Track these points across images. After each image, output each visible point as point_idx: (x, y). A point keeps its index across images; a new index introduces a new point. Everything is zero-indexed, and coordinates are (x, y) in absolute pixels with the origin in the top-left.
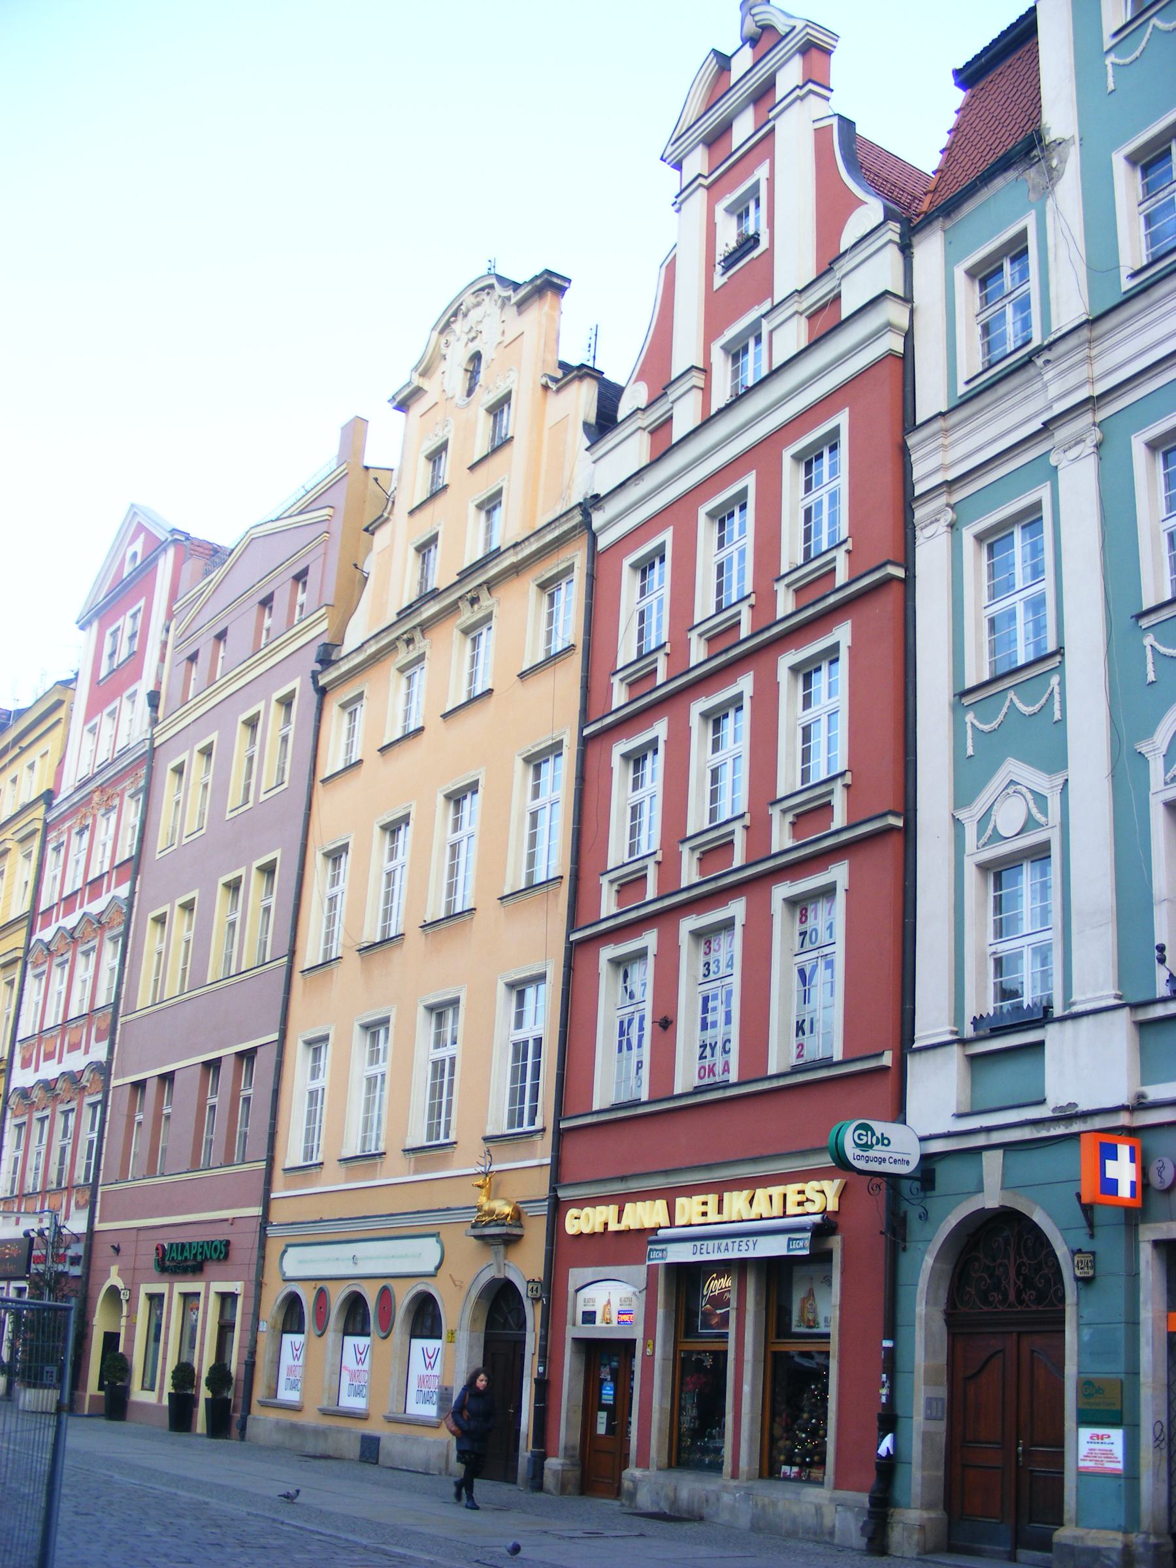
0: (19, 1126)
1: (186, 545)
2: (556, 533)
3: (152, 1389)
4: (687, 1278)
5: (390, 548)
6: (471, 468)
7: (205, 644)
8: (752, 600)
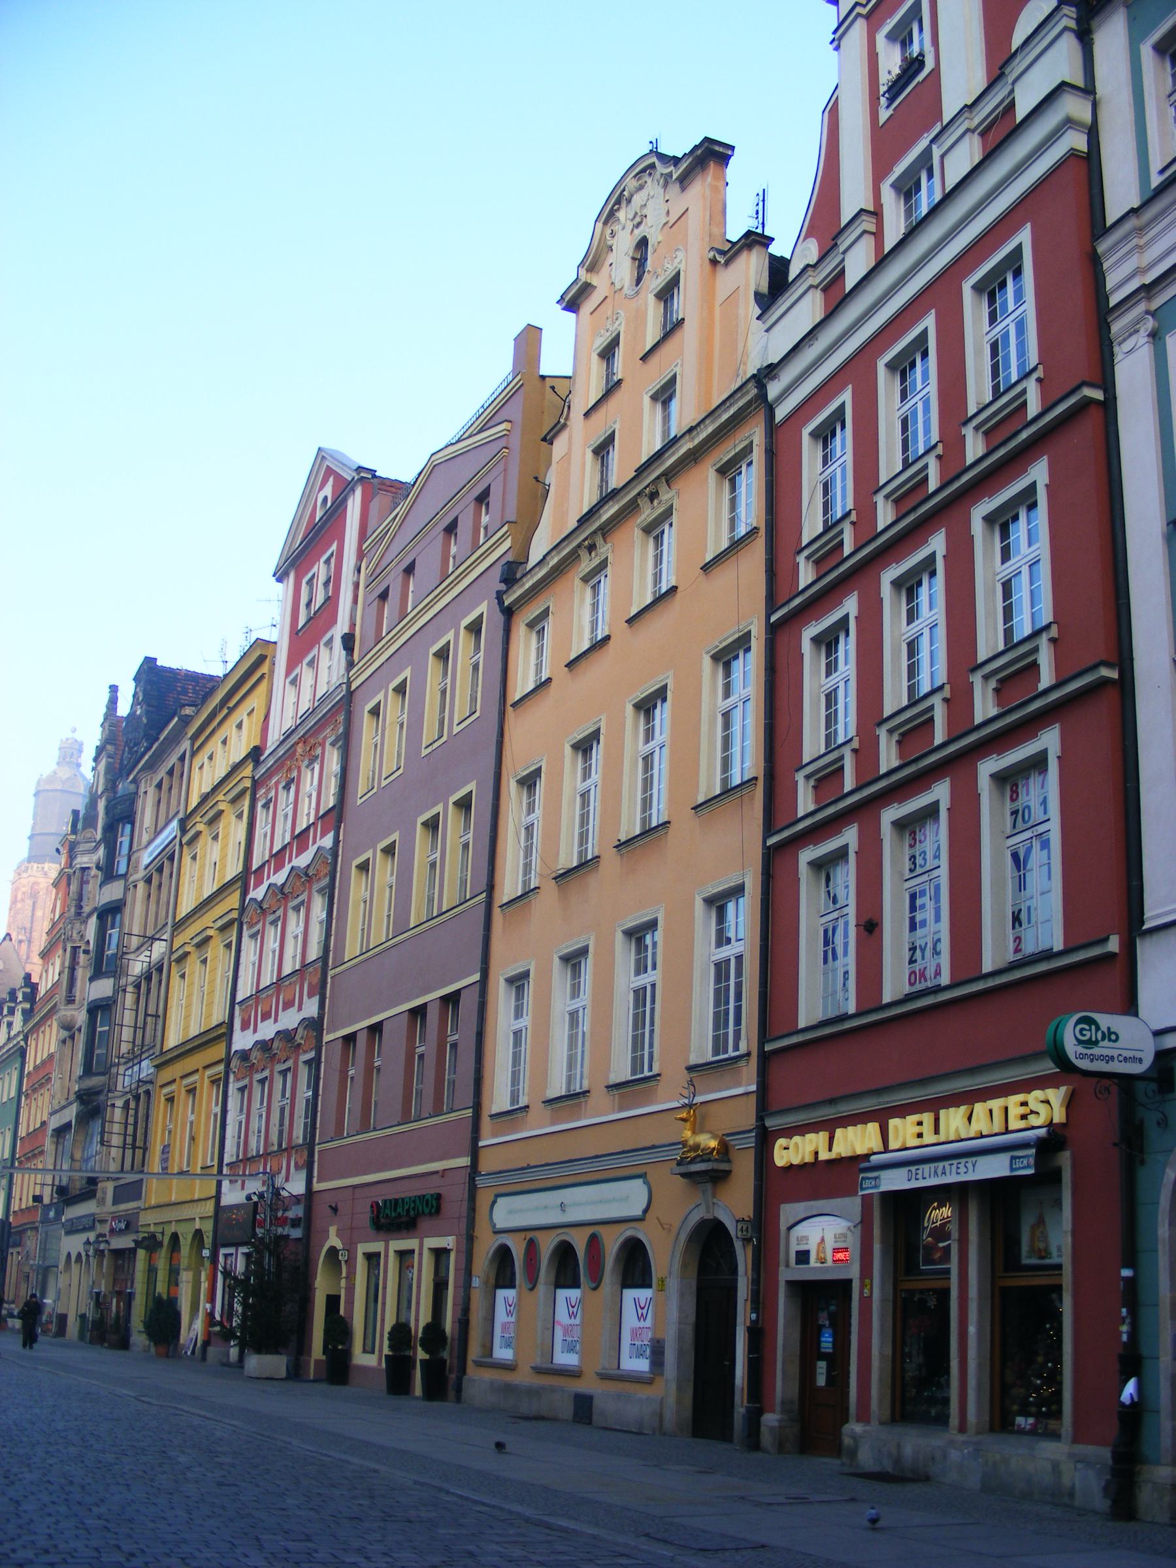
0: (242, 1090)
1: (368, 480)
2: (731, 411)
3: (373, 1352)
4: (904, 1209)
5: (567, 456)
6: (644, 358)
7: (394, 579)
8: (939, 450)
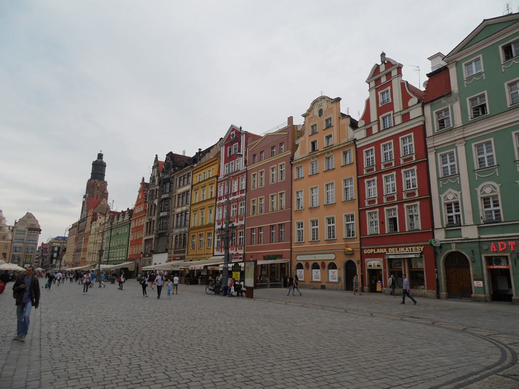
4: (390, 260)
